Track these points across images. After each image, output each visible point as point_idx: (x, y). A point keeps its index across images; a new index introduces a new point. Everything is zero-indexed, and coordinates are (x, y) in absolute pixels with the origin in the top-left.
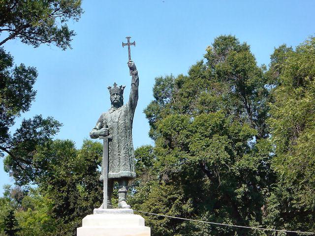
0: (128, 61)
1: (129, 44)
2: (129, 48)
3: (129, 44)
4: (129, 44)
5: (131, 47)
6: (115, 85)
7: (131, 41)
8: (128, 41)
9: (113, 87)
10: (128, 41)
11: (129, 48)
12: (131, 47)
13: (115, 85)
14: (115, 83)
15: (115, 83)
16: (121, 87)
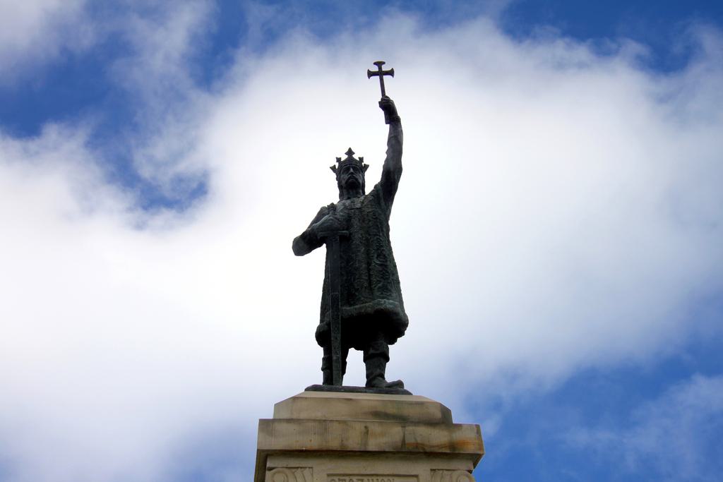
0: (379, 98)
1: (381, 73)
2: (382, 81)
3: (381, 73)
4: (381, 74)
5: (385, 77)
6: (350, 152)
7: (385, 68)
8: (380, 68)
9: (344, 157)
10: (380, 68)
11: (382, 81)
12: (385, 77)
13: (350, 152)
14: (350, 150)
15: (350, 150)
16: (361, 159)
